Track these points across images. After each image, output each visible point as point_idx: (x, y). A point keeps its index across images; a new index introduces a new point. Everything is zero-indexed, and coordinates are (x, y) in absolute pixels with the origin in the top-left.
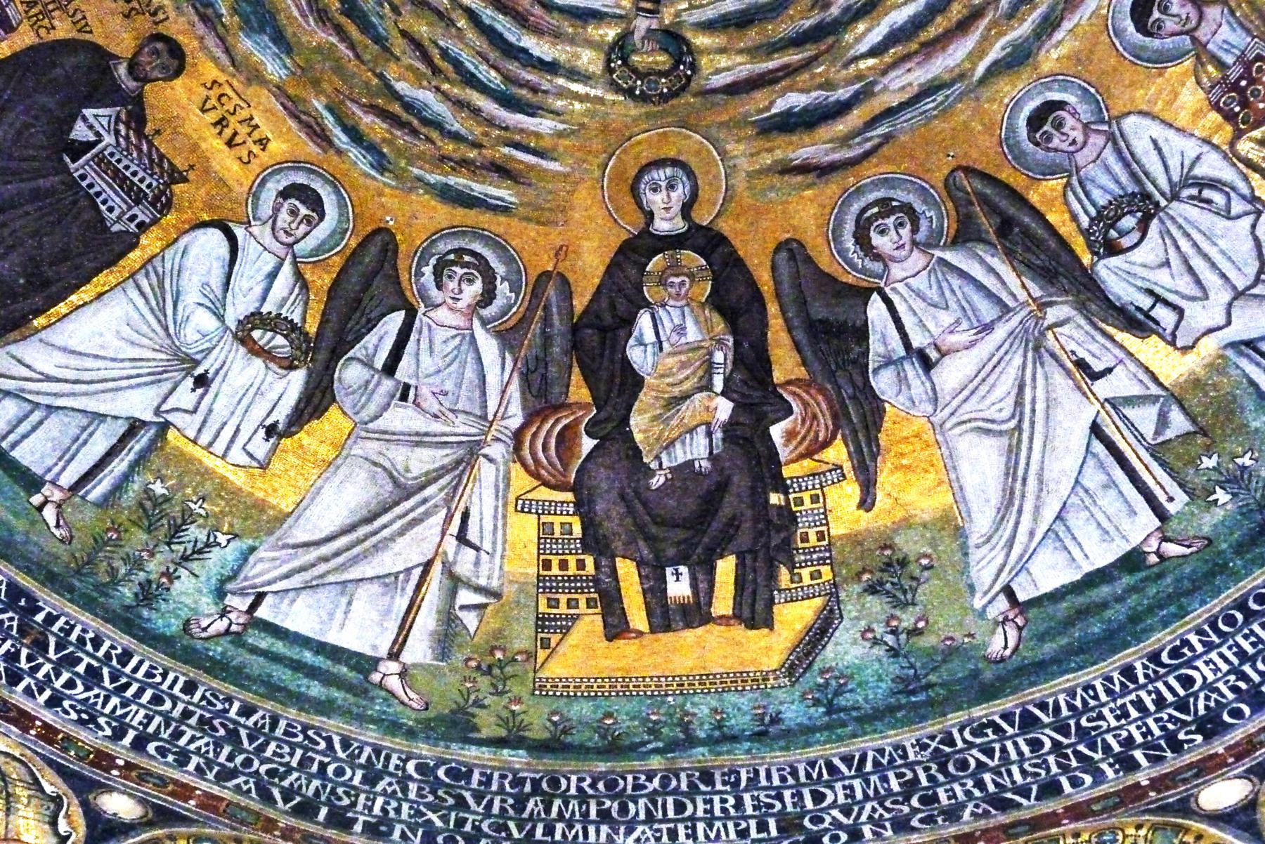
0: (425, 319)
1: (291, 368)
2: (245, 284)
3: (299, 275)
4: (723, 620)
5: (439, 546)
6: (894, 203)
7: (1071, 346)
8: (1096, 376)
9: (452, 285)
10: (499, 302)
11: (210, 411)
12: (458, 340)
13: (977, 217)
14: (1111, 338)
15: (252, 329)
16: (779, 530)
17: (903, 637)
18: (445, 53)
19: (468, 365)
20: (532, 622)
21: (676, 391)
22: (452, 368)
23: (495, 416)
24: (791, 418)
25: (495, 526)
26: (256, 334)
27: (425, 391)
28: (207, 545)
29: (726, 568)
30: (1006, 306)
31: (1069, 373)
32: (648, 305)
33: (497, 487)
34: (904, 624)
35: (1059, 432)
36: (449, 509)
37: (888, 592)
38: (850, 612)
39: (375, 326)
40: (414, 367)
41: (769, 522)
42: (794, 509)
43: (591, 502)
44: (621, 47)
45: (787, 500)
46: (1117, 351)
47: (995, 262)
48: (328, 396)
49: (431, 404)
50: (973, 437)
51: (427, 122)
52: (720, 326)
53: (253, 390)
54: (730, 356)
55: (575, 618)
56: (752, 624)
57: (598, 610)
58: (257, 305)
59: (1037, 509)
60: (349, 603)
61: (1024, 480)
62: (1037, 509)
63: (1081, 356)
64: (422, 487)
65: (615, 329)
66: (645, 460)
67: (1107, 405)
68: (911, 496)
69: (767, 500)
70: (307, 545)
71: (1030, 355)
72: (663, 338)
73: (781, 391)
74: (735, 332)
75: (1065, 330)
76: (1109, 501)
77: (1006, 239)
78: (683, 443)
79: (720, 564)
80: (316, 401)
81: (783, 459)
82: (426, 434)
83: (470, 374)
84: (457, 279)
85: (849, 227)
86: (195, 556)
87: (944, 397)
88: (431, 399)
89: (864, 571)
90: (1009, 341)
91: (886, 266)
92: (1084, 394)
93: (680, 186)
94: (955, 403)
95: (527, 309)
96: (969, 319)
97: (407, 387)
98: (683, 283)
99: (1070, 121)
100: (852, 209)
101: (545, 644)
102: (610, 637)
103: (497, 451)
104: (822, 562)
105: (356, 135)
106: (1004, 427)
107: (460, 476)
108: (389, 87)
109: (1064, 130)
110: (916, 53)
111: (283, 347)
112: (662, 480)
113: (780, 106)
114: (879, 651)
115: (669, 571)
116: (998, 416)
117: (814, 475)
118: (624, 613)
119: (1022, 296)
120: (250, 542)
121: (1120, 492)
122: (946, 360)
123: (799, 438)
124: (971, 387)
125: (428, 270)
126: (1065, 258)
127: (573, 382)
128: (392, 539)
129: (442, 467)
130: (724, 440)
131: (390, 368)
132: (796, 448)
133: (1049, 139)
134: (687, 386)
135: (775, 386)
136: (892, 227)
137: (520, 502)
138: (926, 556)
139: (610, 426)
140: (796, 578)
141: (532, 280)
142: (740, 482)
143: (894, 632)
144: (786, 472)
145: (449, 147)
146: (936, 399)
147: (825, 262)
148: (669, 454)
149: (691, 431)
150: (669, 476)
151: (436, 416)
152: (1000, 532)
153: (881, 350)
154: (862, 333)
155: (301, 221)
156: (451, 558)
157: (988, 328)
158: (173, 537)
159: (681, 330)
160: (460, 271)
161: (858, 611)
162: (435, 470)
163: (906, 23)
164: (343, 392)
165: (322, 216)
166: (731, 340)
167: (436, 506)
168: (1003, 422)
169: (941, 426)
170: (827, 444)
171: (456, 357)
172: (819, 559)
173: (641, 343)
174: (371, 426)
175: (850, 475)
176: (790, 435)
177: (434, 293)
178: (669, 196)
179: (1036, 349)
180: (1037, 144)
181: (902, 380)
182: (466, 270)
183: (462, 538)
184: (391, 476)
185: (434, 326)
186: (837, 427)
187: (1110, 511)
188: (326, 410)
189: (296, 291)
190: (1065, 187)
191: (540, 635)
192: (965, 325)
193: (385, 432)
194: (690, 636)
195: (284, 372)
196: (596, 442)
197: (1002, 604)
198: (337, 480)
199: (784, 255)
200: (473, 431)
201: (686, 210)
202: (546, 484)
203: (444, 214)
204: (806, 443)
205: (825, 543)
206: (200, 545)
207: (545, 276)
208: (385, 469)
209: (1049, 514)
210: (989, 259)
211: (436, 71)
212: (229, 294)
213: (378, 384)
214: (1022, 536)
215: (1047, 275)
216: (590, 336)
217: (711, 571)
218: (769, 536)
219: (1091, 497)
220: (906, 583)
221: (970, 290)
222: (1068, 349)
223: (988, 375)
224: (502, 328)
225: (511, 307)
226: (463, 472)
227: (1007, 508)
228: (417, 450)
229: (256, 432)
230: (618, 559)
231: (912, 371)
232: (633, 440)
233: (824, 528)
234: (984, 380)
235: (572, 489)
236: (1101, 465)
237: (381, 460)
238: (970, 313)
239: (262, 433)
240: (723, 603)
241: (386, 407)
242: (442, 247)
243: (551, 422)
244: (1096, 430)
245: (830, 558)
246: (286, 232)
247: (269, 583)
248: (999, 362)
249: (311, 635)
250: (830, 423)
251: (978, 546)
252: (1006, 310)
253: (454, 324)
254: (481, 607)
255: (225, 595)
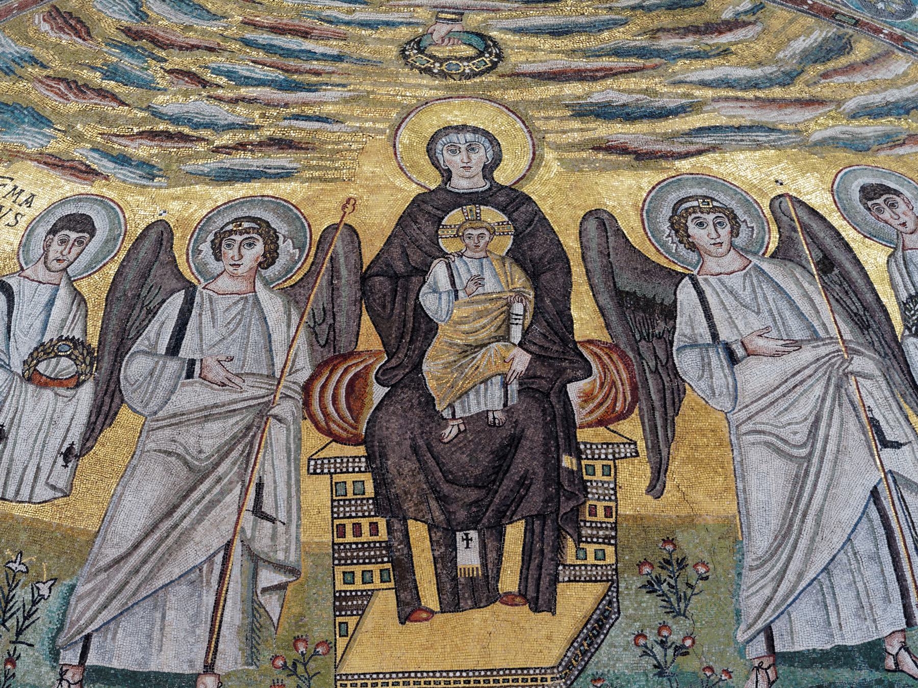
0: (205, 291)
1: (79, 385)
2: (25, 324)
3: (78, 297)
4: (508, 599)
5: (237, 523)
6: (715, 204)
7: (869, 402)
8: (886, 444)
9: (230, 253)
10: (282, 261)
11: (12, 460)
12: (240, 306)
13: (799, 243)
14: (907, 418)
15: (36, 365)
16: (571, 496)
17: (670, 652)
18: (217, 72)
19: (253, 327)
20: (330, 603)
21: (471, 339)
22: (236, 334)
23: (282, 372)
24: (589, 380)
25: (289, 493)
26: (41, 367)
27: (210, 362)
28: (34, 603)
29: (515, 533)
30: (815, 331)
31: (863, 427)
32: (444, 255)
33: (289, 451)
34: (673, 638)
35: (844, 480)
36: (243, 481)
37: (664, 594)
38: (627, 608)
39: (156, 313)
40: (197, 340)
41: (560, 485)
42: (586, 477)
43: (384, 456)
44: (418, 44)
45: (580, 468)
46: (908, 430)
47: (810, 289)
48: (117, 400)
49: (216, 373)
50: (765, 451)
51: (197, 126)
52: (520, 280)
53: (46, 424)
54: (531, 308)
55: (368, 595)
56: (536, 609)
57: (392, 584)
58: (39, 338)
59: (810, 551)
60: (163, 617)
61: (804, 515)
62: (810, 551)
63: (877, 417)
64: (218, 464)
65: (407, 277)
66: (437, 408)
67: (889, 476)
68: (698, 496)
69: (559, 461)
70: (118, 561)
71: (831, 389)
72: (458, 287)
73: (581, 349)
74: (536, 289)
75: (868, 383)
76: (870, 571)
77: (825, 273)
78: (478, 392)
79: (510, 529)
80: (105, 408)
81: (578, 422)
82: (216, 406)
83: (255, 336)
84: (236, 246)
85: (667, 212)
86: (27, 623)
87: (744, 399)
88: (218, 368)
89: (646, 562)
90: (813, 366)
91: (700, 255)
92: (872, 455)
93: (482, 151)
94: (753, 408)
95: (313, 263)
96: (779, 331)
97: (192, 362)
98: (481, 236)
99: (902, 207)
100: (670, 197)
101: (343, 630)
102: (404, 619)
103: (285, 409)
104: (607, 540)
105: (123, 160)
106: (795, 452)
107: (251, 444)
108: (157, 115)
109: (898, 211)
110: (750, 100)
111: (68, 368)
112: (455, 431)
113: (597, 98)
114: (648, 663)
115: (459, 535)
116: (792, 439)
117: (608, 444)
118: (416, 588)
119: (834, 332)
120: (68, 582)
121: (882, 571)
122: (752, 360)
123: (597, 401)
124: (772, 397)
125: (206, 247)
126: (879, 315)
127: (363, 331)
128: (192, 527)
129: (233, 437)
130: (519, 392)
131: (174, 349)
132: (591, 412)
133: (880, 210)
134: (483, 335)
135: (575, 343)
136: (711, 223)
137: (312, 463)
138: (704, 564)
139: (401, 374)
140: (581, 555)
141: (316, 238)
142: (534, 435)
143: (662, 643)
144: (583, 435)
145: (226, 139)
146: (736, 398)
147: (637, 238)
148: (462, 403)
149: (485, 381)
150: (462, 428)
151: (224, 385)
152: (773, 561)
153: (688, 331)
154: (670, 313)
155: (73, 244)
156: (249, 533)
157: (797, 345)
158: (4, 612)
159: (478, 281)
160: (239, 238)
161: (635, 610)
162: (226, 444)
163: (740, 79)
164: (130, 388)
165: (92, 232)
166: (532, 293)
167: (231, 483)
168: (794, 446)
169: (737, 427)
170: (623, 416)
171: (240, 320)
172: (606, 537)
173: (435, 291)
174: (161, 414)
175: (643, 452)
176: (587, 397)
177: (215, 266)
178: (469, 157)
179: (838, 387)
180: (869, 209)
181: (706, 365)
182: (246, 236)
183: (258, 511)
184: (186, 463)
185: (215, 295)
186: (635, 399)
187: (871, 585)
188: (116, 414)
189: (75, 308)
190: (890, 256)
191: (339, 620)
192: (774, 334)
193: (175, 415)
194: (477, 617)
195: (73, 392)
196: (387, 390)
197: (759, 647)
198: (134, 483)
199: (592, 224)
200: (262, 392)
201: (488, 170)
202: (337, 439)
203: (223, 194)
204: (603, 409)
205: (612, 520)
206: (28, 607)
207: (334, 228)
208: (178, 456)
209: (821, 560)
210: (806, 285)
211: (204, 84)
212: (12, 343)
213: (164, 366)
214: (790, 576)
215: (862, 324)
216: (380, 284)
217: (501, 536)
218: (559, 501)
219: (857, 560)
220: (682, 587)
221: (784, 305)
222: (867, 404)
223: (790, 391)
224: (286, 285)
225: (297, 263)
226: (254, 436)
227: (784, 537)
228: (208, 425)
229: (55, 462)
230: (410, 522)
231: (717, 359)
232: (424, 387)
233: (612, 504)
234: (784, 396)
235: (364, 442)
236: (873, 530)
237: (172, 447)
238: (780, 323)
239: (60, 461)
240: (509, 581)
241: (172, 392)
242: (219, 223)
243: (340, 372)
244: (875, 494)
245: (615, 537)
246: (58, 260)
247: (92, 620)
248: (802, 382)
249: (135, 668)
250: (628, 394)
251: (751, 569)
252: (815, 337)
253: (235, 290)
254: (281, 587)
255: (58, 654)
